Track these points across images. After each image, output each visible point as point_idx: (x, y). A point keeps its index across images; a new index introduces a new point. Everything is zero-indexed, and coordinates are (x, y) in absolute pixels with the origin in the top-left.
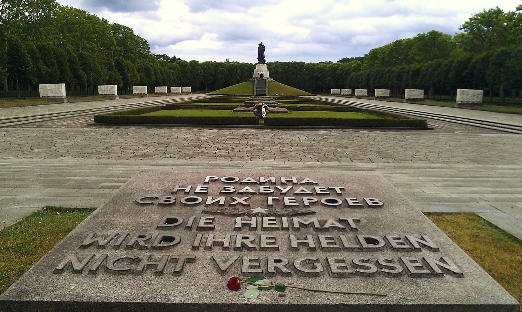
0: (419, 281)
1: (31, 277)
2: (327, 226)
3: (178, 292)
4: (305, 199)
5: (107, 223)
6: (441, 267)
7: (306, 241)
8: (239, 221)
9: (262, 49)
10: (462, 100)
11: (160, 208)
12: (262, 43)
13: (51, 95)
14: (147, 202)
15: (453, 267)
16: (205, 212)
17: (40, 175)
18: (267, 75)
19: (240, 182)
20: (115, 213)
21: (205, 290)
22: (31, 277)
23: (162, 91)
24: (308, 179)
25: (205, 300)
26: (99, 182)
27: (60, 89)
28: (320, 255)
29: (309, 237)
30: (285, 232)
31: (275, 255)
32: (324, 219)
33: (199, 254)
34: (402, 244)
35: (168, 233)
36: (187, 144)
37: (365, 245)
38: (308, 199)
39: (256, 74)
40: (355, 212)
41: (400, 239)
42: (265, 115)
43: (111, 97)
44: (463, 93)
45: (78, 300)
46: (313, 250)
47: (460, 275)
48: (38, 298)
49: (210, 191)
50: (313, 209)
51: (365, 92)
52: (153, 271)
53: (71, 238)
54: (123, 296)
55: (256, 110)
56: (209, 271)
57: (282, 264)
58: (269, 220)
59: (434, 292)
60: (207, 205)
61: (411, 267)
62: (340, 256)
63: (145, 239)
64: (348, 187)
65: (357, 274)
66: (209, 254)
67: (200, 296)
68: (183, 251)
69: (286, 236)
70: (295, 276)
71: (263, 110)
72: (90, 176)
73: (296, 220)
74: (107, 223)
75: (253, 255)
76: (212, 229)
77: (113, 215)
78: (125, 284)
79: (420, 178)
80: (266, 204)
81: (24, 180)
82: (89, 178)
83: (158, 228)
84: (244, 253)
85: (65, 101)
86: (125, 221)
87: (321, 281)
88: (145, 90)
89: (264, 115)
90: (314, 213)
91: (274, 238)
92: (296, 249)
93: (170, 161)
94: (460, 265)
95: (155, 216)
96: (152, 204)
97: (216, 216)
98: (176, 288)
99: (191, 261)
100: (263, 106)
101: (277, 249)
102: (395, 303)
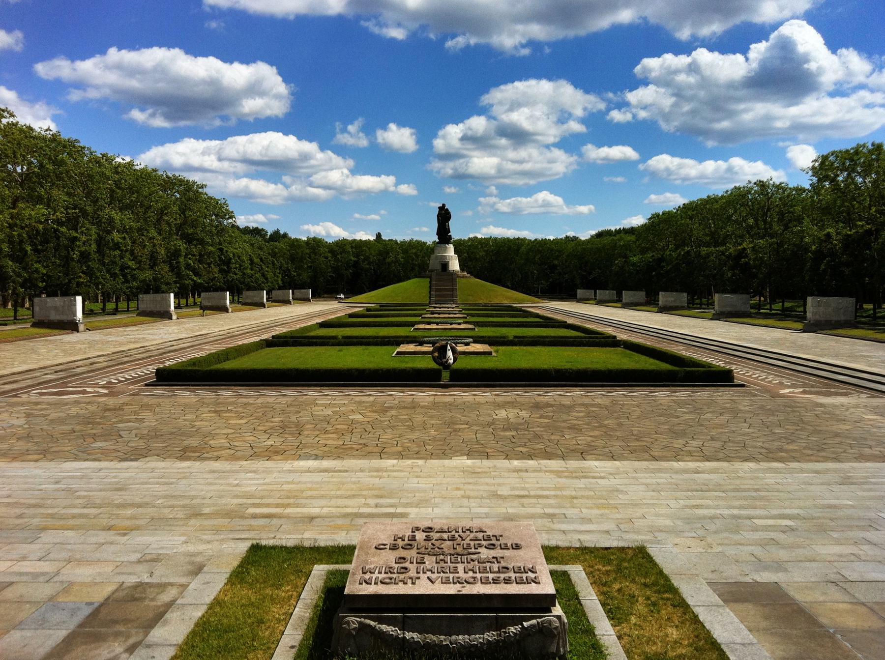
9: (444, 216)
10: (817, 317)
12: (444, 205)
23: (256, 299)
28: (478, 575)
31: (457, 575)
33: (421, 575)
36: (329, 428)
39: (434, 264)
42: (451, 361)
44: (819, 304)
50: (479, 550)
51: (641, 295)
62: (487, 575)
64: (506, 534)
66: (426, 576)
71: (450, 354)
75: (447, 575)
84: (442, 574)
88: (226, 299)
93: (311, 464)
99: (419, 578)
100: (449, 347)
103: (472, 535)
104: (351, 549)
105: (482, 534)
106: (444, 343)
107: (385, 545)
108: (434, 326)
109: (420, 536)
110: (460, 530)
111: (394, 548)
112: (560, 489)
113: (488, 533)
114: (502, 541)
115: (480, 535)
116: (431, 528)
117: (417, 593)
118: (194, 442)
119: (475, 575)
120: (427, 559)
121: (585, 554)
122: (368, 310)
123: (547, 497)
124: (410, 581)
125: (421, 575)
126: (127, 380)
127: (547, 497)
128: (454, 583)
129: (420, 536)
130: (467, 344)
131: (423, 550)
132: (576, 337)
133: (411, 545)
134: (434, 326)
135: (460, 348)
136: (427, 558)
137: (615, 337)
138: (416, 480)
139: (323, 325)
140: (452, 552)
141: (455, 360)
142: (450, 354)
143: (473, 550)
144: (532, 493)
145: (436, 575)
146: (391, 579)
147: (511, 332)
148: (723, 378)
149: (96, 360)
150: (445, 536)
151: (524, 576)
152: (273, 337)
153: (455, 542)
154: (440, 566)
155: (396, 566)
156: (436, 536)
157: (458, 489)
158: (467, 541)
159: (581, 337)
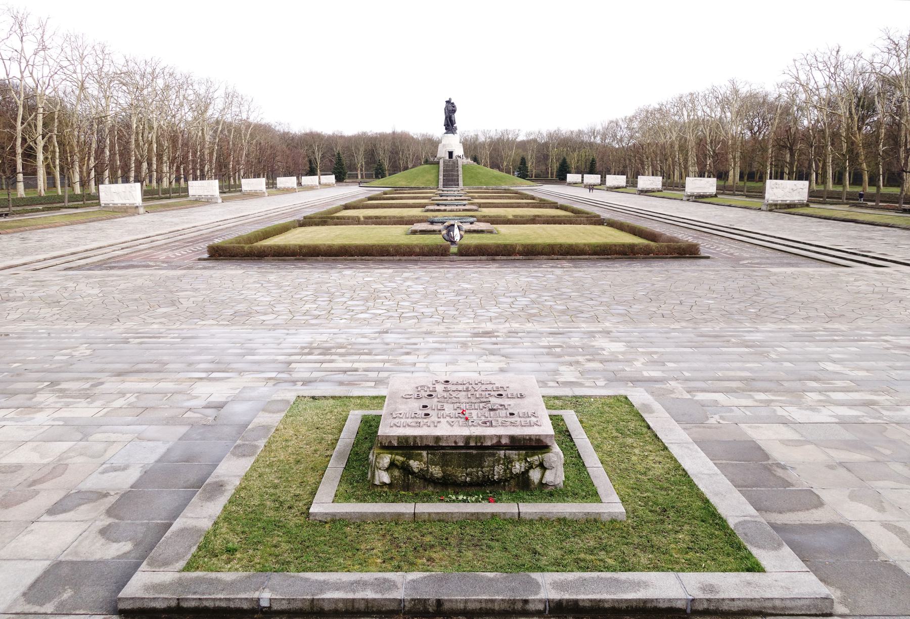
8: (456, 406)
9: (450, 110)
13: (118, 201)
14: (407, 398)
18: (459, 151)
27: (132, 193)
39: (442, 153)
43: (208, 201)
51: (621, 180)
55: (444, 232)
64: (511, 385)
66: (445, 420)
71: (456, 231)
73: (482, 405)
85: (142, 210)
89: (457, 238)
95: (416, 405)
99: (439, 422)
103: (484, 387)
104: (383, 398)
106: (452, 222)
108: (443, 208)
109: (440, 388)
111: (418, 398)
114: (509, 392)
115: (489, 387)
118: (241, 307)
120: (446, 406)
121: (576, 402)
122: (385, 193)
124: (432, 425)
125: (442, 420)
126: (183, 255)
129: (440, 388)
130: (472, 223)
132: (566, 216)
134: (443, 208)
135: (466, 227)
136: (446, 406)
137: (599, 216)
139: (346, 207)
140: (467, 401)
141: (462, 237)
142: (456, 231)
147: (510, 213)
148: (688, 253)
149: (155, 238)
150: (460, 388)
151: (528, 420)
152: (305, 218)
153: (469, 393)
155: (420, 412)
159: (569, 217)
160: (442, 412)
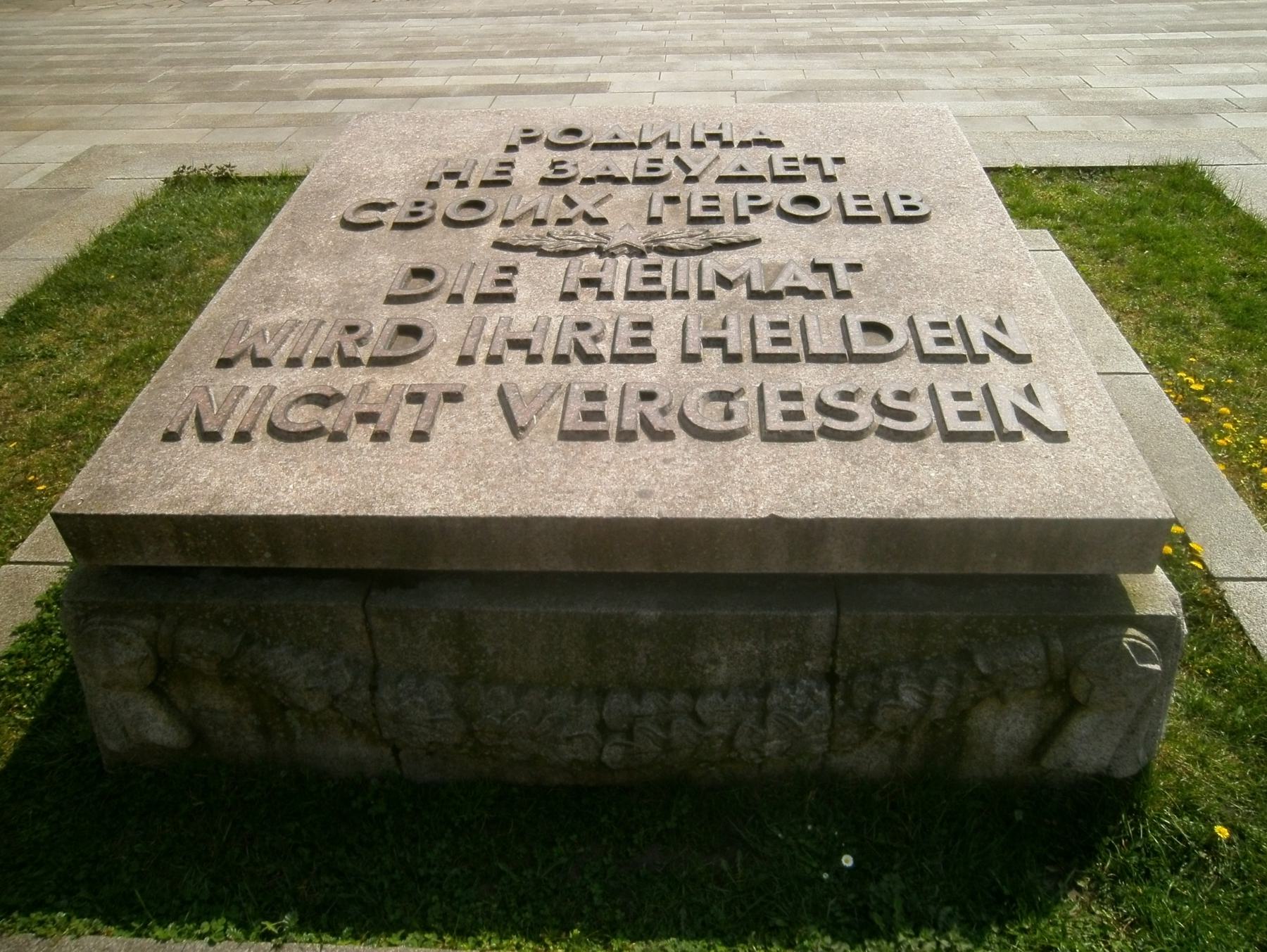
0: (963, 448)
1: (117, 451)
2: (778, 286)
3: (419, 488)
4: (744, 190)
5: (280, 286)
6: (1022, 416)
7: (721, 334)
11: (398, 233)
15: (1050, 417)
16: (499, 245)
17: (171, 63)
19: (594, 140)
20: (295, 255)
21: (478, 478)
22: (117, 451)
24: (760, 128)
25: (473, 509)
26: (307, 78)
28: (749, 375)
29: (732, 322)
30: (679, 302)
31: (644, 376)
32: (780, 258)
34: (948, 341)
35: (407, 314)
37: (860, 343)
38: (752, 198)
40: (858, 235)
41: (944, 325)
45: (215, 511)
46: (735, 358)
47: (1061, 437)
48: (134, 508)
49: (518, 173)
52: (371, 427)
53: (198, 334)
54: (306, 501)
56: (492, 426)
57: (657, 404)
58: (647, 267)
59: (989, 484)
60: (506, 223)
61: (951, 409)
63: (357, 335)
65: (826, 432)
66: (497, 376)
67: (466, 499)
68: (438, 369)
69: (679, 316)
70: (682, 437)
72: (287, 60)
73: (712, 263)
74: (280, 286)
76: (509, 298)
77: (292, 261)
78: (311, 466)
79: (1090, 37)
80: (645, 215)
81: (138, 79)
82: (283, 67)
83: (391, 300)
86: (319, 279)
87: (739, 454)
90: (756, 241)
91: (647, 325)
92: (695, 358)
94: (1069, 403)
95: (385, 260)
96: (379, 224)
97: (523, 255)
98: (417, 476)
99: (453, 397)
101: (650, 358)
102: (892, 515)
105: (765, 152)
107: (381, 207)
110: (685, 140)
112: (902, 34)
113: (789, 151)
115: (756, 161)
116: (577, 132)
117: (420, 506)
119: (728, 378)
123: (876, 48)
127: (876, 48)
128: (626, 436)
129: (531, 164)
131: (524, 232)
133: (480, 205)
138: (639, 25)
143: (728, 230)
144: (849, 42)
145: (546, 371)
146: (323, 401)
150: (623, 163)
153: (660, 191)
154: (572, 311)
156: (587, 162)
157: (712, 37)
158: (709, 185)
160: (496, 313)
